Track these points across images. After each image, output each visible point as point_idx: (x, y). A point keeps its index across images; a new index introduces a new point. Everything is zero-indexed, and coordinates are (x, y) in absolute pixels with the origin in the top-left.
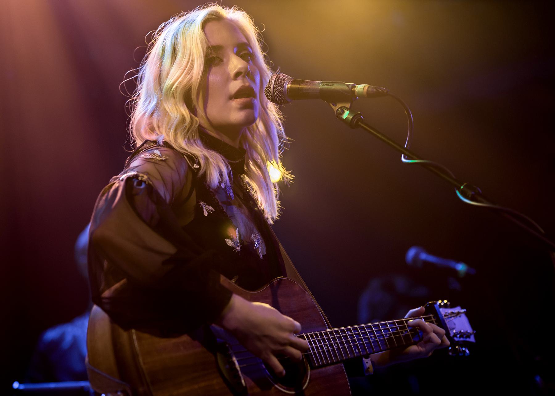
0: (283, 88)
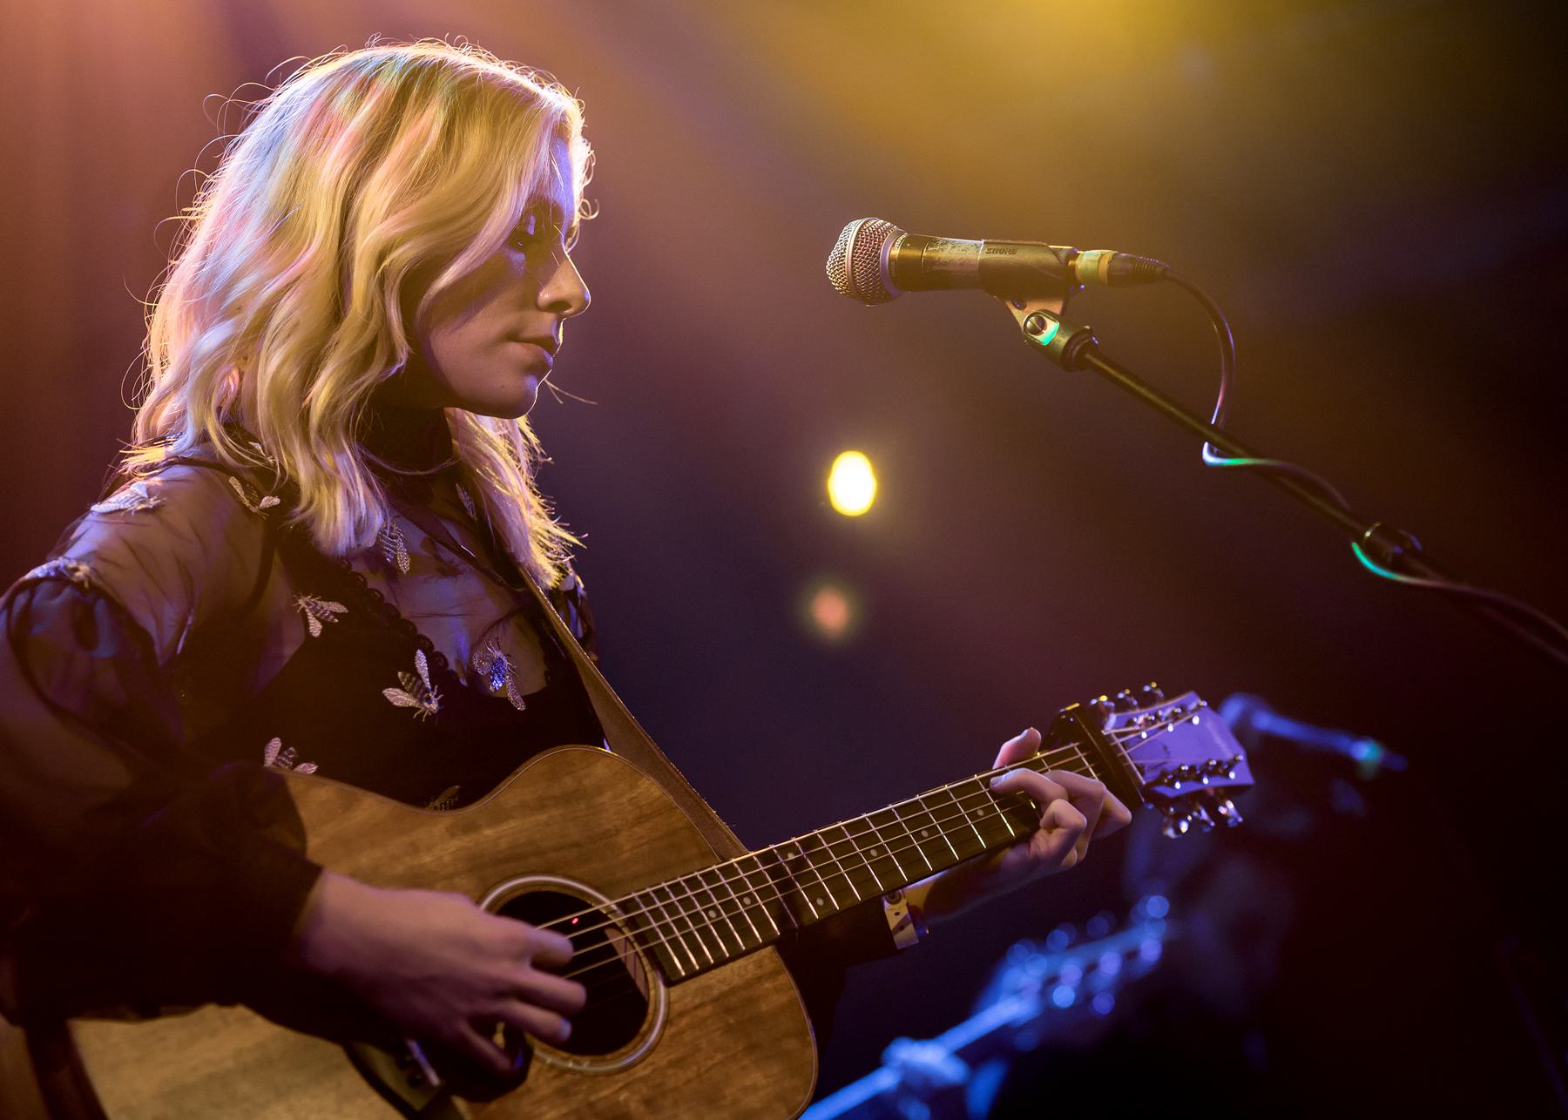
0: (878, 258)
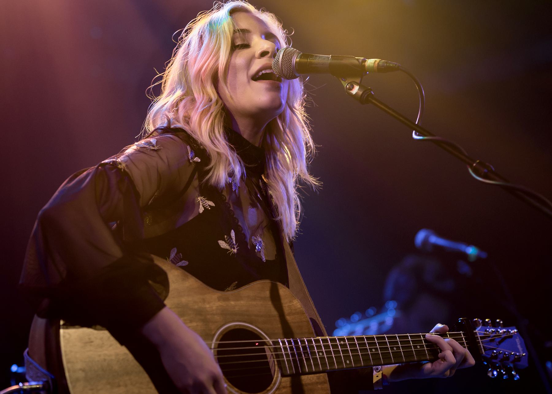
0: (291, 62)
